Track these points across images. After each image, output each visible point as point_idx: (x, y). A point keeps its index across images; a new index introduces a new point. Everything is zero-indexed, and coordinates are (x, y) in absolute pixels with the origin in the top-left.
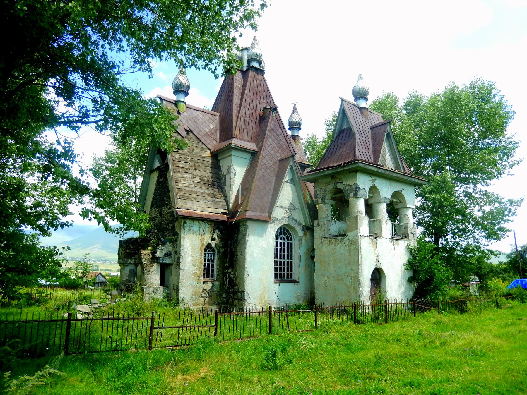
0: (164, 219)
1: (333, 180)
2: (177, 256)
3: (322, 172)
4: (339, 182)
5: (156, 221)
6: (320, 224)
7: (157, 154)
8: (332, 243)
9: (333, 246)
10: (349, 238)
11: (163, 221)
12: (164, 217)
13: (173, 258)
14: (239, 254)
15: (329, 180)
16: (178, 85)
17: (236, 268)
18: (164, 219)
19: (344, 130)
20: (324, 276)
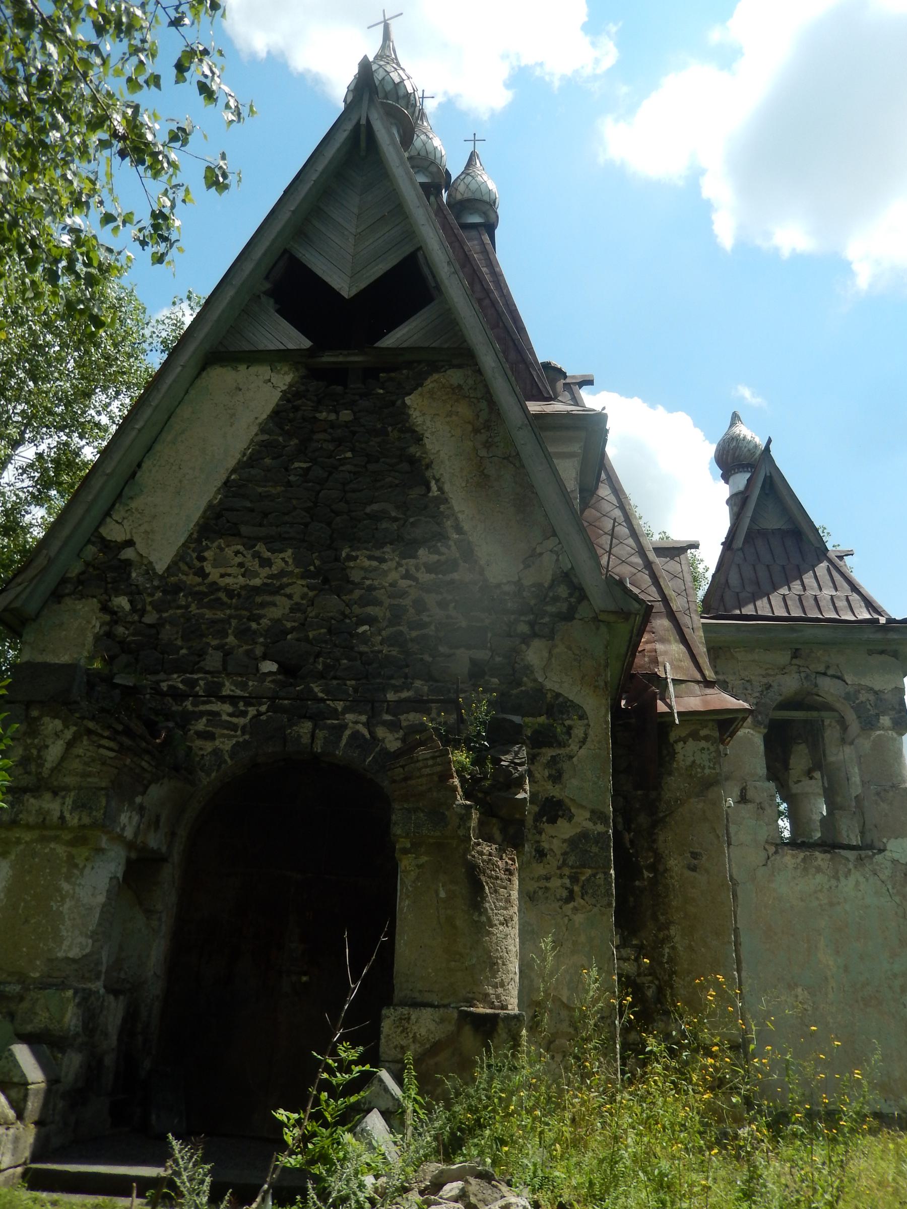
1: (795, 661)
2: (564, 830)
3: (792, 629)
4: (825, 674)
6: (750, 794)
7: (270, 293)
8: (819, 870)
9: (819, 878)
10: (896, 856)
12: (377, 603)
14: (675, 864)
15: (783, 658)
16: (401, 93)
17: (666, 926)
19: (764, 534)
20: (791, 987)
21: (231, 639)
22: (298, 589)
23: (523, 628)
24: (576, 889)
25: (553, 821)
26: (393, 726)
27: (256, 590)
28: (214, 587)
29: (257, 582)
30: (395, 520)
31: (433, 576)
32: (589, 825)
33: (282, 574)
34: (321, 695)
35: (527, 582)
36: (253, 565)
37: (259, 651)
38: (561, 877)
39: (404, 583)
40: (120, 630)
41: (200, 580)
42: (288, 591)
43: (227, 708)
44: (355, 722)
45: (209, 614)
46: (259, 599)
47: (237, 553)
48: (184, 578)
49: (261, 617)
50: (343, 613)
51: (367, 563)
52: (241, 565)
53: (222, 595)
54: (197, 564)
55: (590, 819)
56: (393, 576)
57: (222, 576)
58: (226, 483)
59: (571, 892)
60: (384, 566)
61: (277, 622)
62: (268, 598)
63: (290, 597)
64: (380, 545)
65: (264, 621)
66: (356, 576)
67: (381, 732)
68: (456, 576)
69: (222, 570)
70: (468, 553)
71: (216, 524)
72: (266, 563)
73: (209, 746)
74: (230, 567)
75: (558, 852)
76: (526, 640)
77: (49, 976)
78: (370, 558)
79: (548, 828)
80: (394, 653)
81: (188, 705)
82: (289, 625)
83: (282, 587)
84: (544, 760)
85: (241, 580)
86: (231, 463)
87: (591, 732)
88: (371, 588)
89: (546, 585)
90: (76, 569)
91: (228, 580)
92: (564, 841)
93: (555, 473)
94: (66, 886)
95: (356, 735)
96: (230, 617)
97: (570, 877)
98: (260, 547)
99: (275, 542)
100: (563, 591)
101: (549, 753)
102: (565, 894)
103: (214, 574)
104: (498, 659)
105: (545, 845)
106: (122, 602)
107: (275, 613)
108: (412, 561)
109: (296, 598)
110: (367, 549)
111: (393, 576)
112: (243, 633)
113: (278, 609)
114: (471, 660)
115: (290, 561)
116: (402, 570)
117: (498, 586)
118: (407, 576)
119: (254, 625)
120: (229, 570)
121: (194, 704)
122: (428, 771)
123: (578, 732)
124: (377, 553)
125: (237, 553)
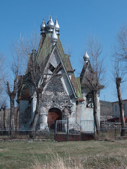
0: (59, 97)
12: (59, 96)
18: (59, 97)
21: (49, 99)
22: (53, 95)
23: (70, 99)
26: (61, 106)
28: (47, 95)
33: (52, 94)
36: (50, 93)
37: (51, 100)
39: (61, 95)
43: (49, 104)
44: (59, 105)
56: (61, 94)
64: (59, 92)
66: (58, 94)
67: (60, 106)
72: (51, 93)
73: (48, 107)
76: (70, 99)
93: (69, 77)
95: (59, 107)
98: (50, 92)
99: (51, 91)
100: (73, 96)
103: (47, 94)
112: (50, 99)
113: (52, 97)
118: (61, 94)
123: (74, 106)
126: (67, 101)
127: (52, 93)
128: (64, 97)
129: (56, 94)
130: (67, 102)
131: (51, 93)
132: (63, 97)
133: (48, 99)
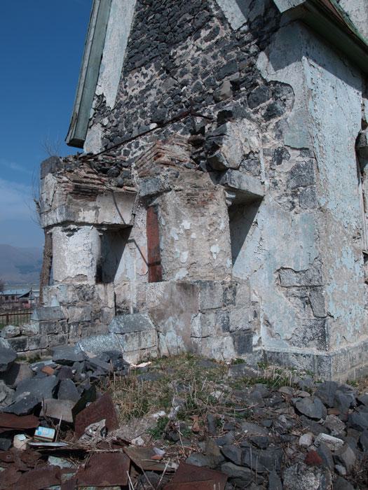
0: (188, 77)
5: (151, 99)
11: (185, 84)
13: (263, 175)
21: (140, 119)
24: (296, 200)
25: (279, 163)
27: (143, 92)
28: (131, 98)
29: (144, 87)
30: (189, 21)
31: (209, 43)
32: (300, 159)
33: (152, 77)
34: (172, 131)
35: (251, 20)
36: (141, 79)
37: (149, 120)
38: (287, 195)
40: (108, 133)
41: (126, 97)
42: (154, 85)
45: (131, 111)
46: (145, 96)
47: (136, 77)
48: (121, 99)
49: (147, 103)
50: (175, 85)
51: (180, 53)
52: (138, 82)
53: (134, 100)
54: (124, 90)
55: (300, 155)
57: (133, 91)
58: (128, 43)
59: (293, 203)
60: (188, 50)
61: (153, 102)
62: (148, 93)
63: (155, 88)
65: (149, 105)
68: (218, 37)
69: (132, 89)
70: (223, 19)
71: (130, 67)
74: (137, 83)
75: (284, 182)
76: (256, 55)
77: (105, 275)
78: (181, 49)
79: (277, 168)
80: (197, 96)
81: (130, 157)
82: (157, 102)
83: (152, 85)
84: (271, 127)
85: (139, 89)
86: (128, 34)
87: (296, 99)
88: (185, 65)
89: (262, 14)
90: (92, 111)
91: (136, 92)
92: (287, 173)
94: (64, 246)
96: (137, 109)
97: (292, 195)
101: (274, 121)
102: (290, 205)
104: (243, 75)
105: (277, 179)
106: (106, 121)
107: (151, 99)
108: (198, 41)
109: (158, 87)
110: (181, 45)
111: (193, 52)
112: (143, 114)
114: (231, 82)
115: (153, 70)
116: (195, 48)
117: (239, 30)
118: (199, 49)
119: (146, 109)
120: (134, 87)
121: (132, 155)
122: (149, 157)
123: (289, 102)
124: (184, 45)
125: (136, 77)
126: (236, 76)
127: (151, 71)
128: (214, 57)
129: (169, 70)
130: (236, 86)
131: (145, 75)
132: (205, 62)
133: (137, 118)
